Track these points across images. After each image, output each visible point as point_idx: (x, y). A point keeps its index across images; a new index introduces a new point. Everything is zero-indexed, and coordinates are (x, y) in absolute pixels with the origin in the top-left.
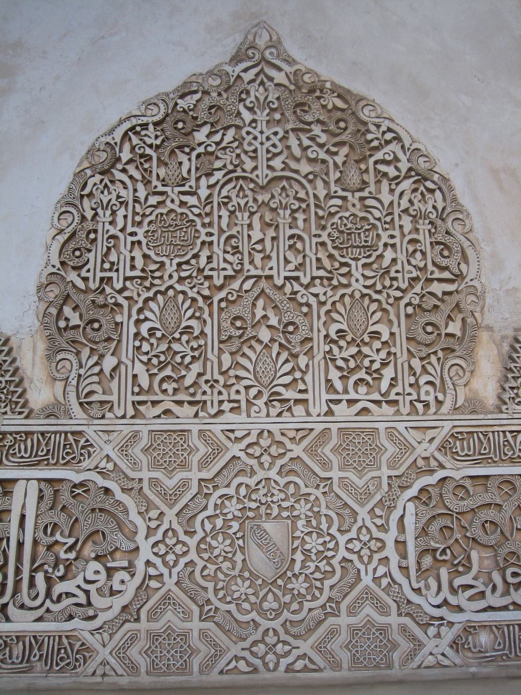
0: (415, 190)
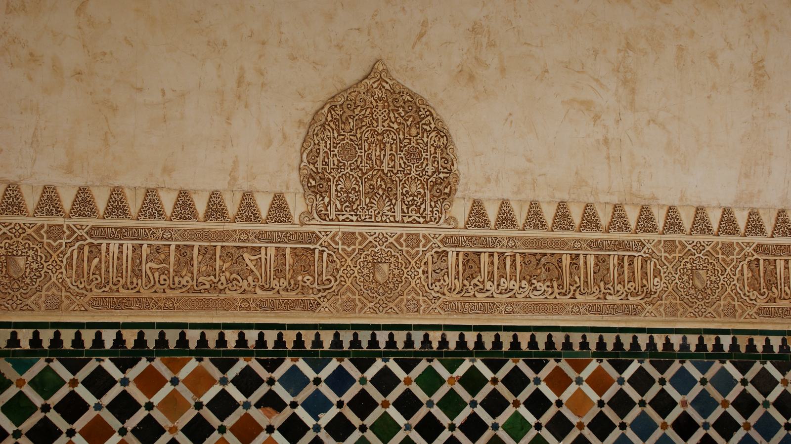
0: (436, 136)
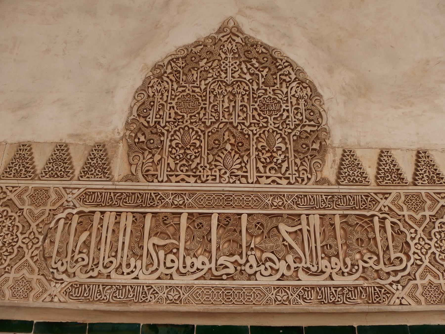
0: (298, 87)
